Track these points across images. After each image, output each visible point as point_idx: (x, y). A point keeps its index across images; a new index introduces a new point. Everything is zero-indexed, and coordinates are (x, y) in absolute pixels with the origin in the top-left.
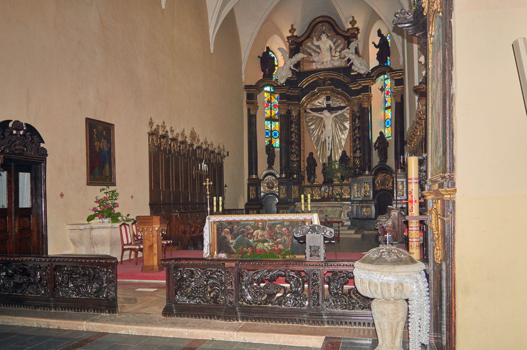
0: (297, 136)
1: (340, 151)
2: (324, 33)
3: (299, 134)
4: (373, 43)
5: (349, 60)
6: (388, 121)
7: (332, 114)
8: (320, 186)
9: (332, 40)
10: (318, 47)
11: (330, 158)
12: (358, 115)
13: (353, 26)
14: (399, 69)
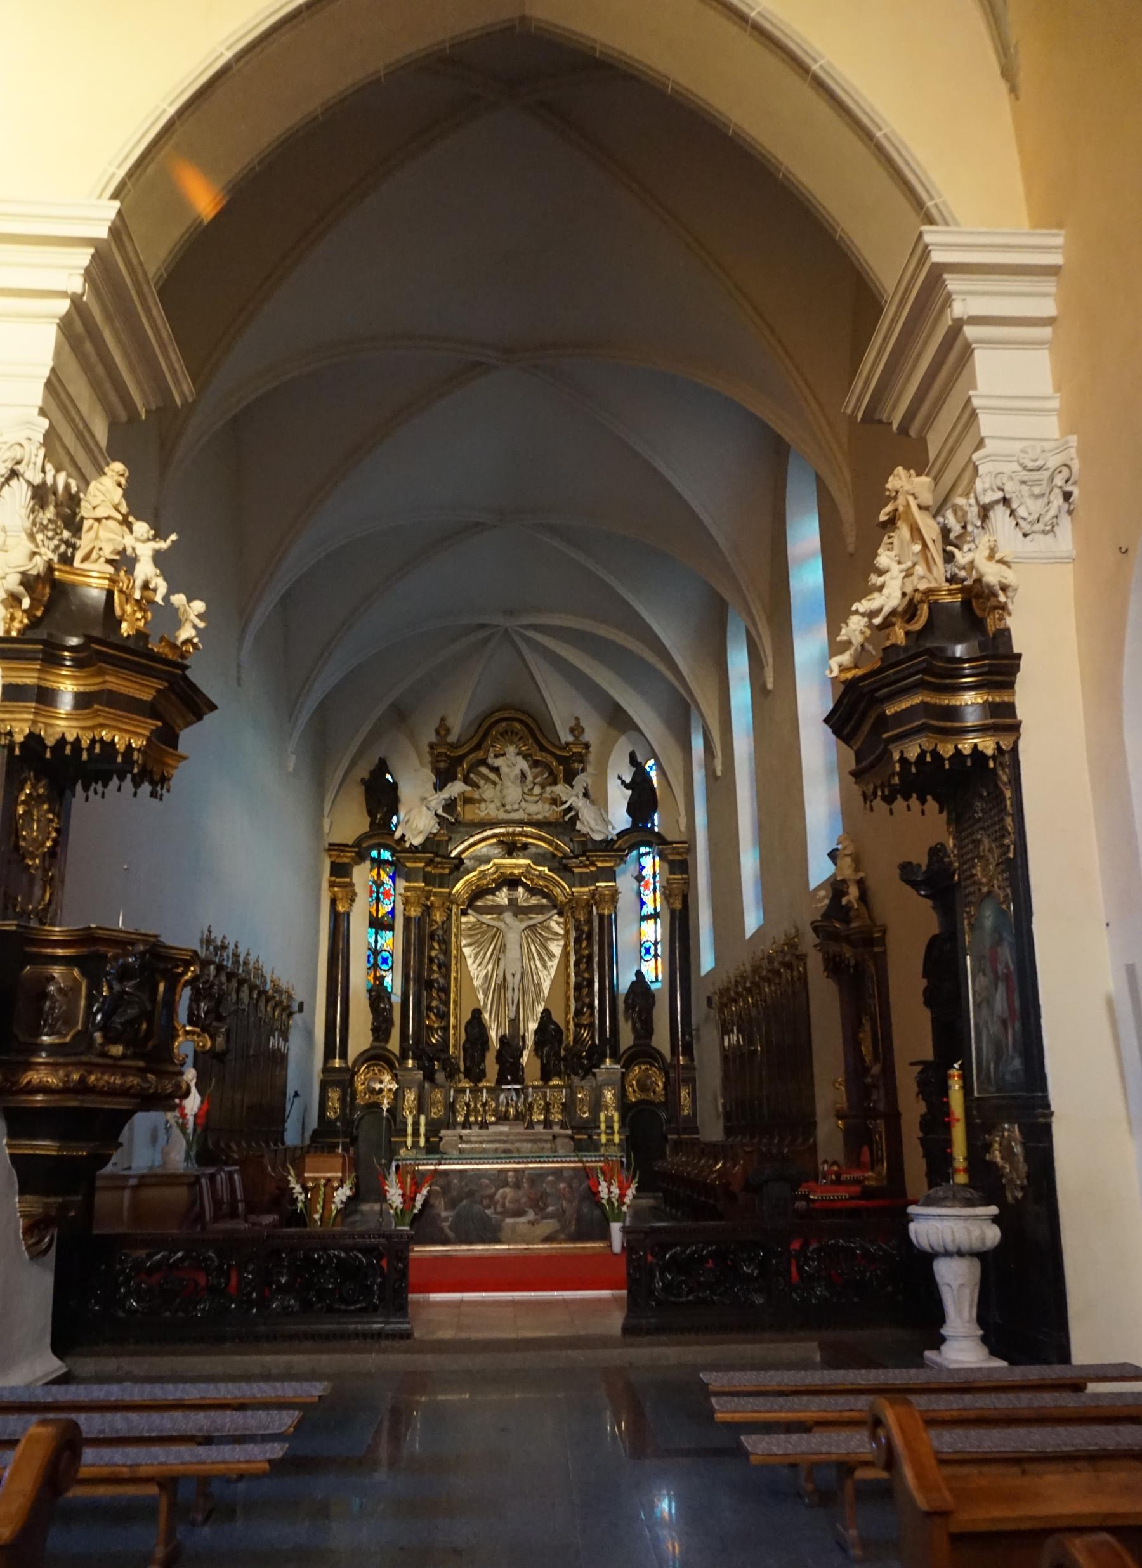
0: (444, 970)
1: (540, 1009)
2: (512, 743)
3: (445, 967)
4: (620, 778)
5: (570, 809)
6: (647, 945)
7: (521, 921)
8: (494, 1091)
9: (525, 756)
10: (496, 770)
11: (514, 1023)
12: (586, 929)
13: (576, 737)
14: (677, 839)
